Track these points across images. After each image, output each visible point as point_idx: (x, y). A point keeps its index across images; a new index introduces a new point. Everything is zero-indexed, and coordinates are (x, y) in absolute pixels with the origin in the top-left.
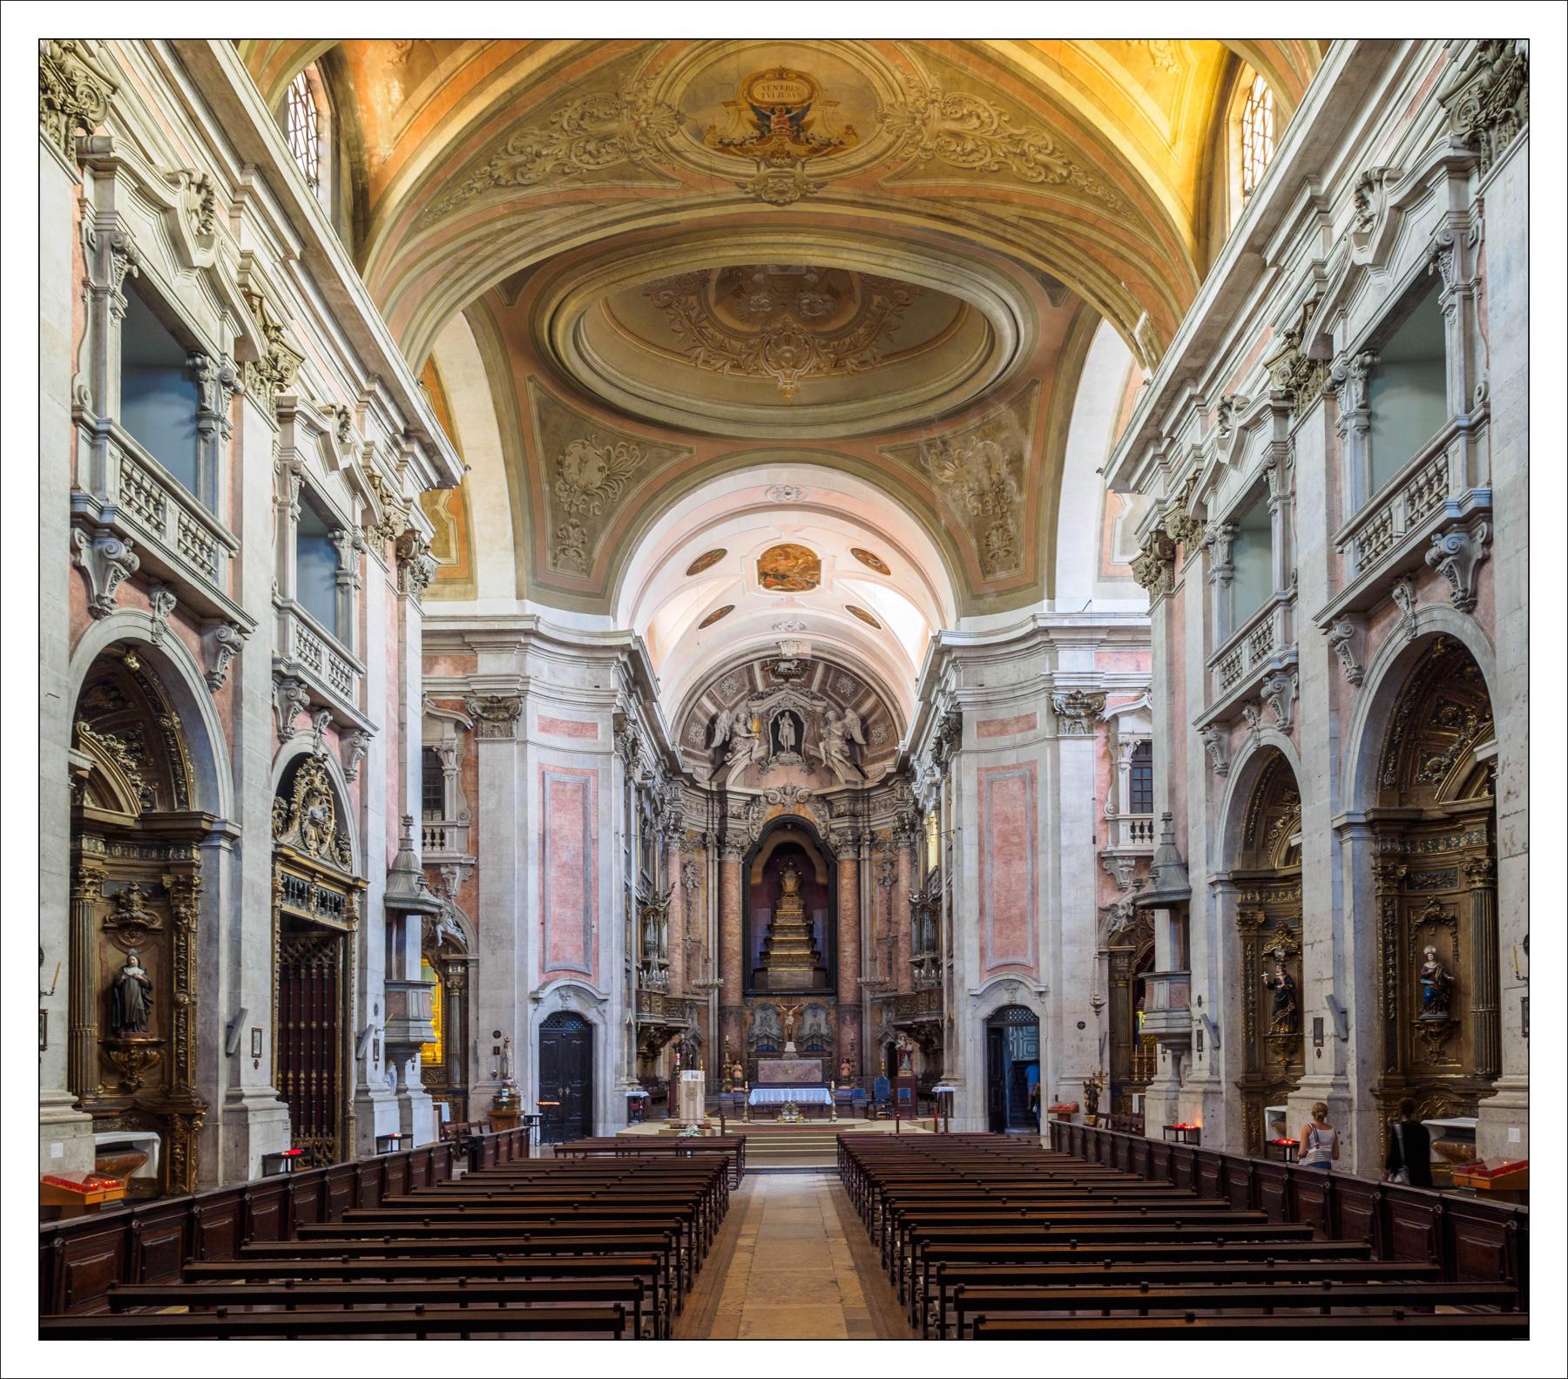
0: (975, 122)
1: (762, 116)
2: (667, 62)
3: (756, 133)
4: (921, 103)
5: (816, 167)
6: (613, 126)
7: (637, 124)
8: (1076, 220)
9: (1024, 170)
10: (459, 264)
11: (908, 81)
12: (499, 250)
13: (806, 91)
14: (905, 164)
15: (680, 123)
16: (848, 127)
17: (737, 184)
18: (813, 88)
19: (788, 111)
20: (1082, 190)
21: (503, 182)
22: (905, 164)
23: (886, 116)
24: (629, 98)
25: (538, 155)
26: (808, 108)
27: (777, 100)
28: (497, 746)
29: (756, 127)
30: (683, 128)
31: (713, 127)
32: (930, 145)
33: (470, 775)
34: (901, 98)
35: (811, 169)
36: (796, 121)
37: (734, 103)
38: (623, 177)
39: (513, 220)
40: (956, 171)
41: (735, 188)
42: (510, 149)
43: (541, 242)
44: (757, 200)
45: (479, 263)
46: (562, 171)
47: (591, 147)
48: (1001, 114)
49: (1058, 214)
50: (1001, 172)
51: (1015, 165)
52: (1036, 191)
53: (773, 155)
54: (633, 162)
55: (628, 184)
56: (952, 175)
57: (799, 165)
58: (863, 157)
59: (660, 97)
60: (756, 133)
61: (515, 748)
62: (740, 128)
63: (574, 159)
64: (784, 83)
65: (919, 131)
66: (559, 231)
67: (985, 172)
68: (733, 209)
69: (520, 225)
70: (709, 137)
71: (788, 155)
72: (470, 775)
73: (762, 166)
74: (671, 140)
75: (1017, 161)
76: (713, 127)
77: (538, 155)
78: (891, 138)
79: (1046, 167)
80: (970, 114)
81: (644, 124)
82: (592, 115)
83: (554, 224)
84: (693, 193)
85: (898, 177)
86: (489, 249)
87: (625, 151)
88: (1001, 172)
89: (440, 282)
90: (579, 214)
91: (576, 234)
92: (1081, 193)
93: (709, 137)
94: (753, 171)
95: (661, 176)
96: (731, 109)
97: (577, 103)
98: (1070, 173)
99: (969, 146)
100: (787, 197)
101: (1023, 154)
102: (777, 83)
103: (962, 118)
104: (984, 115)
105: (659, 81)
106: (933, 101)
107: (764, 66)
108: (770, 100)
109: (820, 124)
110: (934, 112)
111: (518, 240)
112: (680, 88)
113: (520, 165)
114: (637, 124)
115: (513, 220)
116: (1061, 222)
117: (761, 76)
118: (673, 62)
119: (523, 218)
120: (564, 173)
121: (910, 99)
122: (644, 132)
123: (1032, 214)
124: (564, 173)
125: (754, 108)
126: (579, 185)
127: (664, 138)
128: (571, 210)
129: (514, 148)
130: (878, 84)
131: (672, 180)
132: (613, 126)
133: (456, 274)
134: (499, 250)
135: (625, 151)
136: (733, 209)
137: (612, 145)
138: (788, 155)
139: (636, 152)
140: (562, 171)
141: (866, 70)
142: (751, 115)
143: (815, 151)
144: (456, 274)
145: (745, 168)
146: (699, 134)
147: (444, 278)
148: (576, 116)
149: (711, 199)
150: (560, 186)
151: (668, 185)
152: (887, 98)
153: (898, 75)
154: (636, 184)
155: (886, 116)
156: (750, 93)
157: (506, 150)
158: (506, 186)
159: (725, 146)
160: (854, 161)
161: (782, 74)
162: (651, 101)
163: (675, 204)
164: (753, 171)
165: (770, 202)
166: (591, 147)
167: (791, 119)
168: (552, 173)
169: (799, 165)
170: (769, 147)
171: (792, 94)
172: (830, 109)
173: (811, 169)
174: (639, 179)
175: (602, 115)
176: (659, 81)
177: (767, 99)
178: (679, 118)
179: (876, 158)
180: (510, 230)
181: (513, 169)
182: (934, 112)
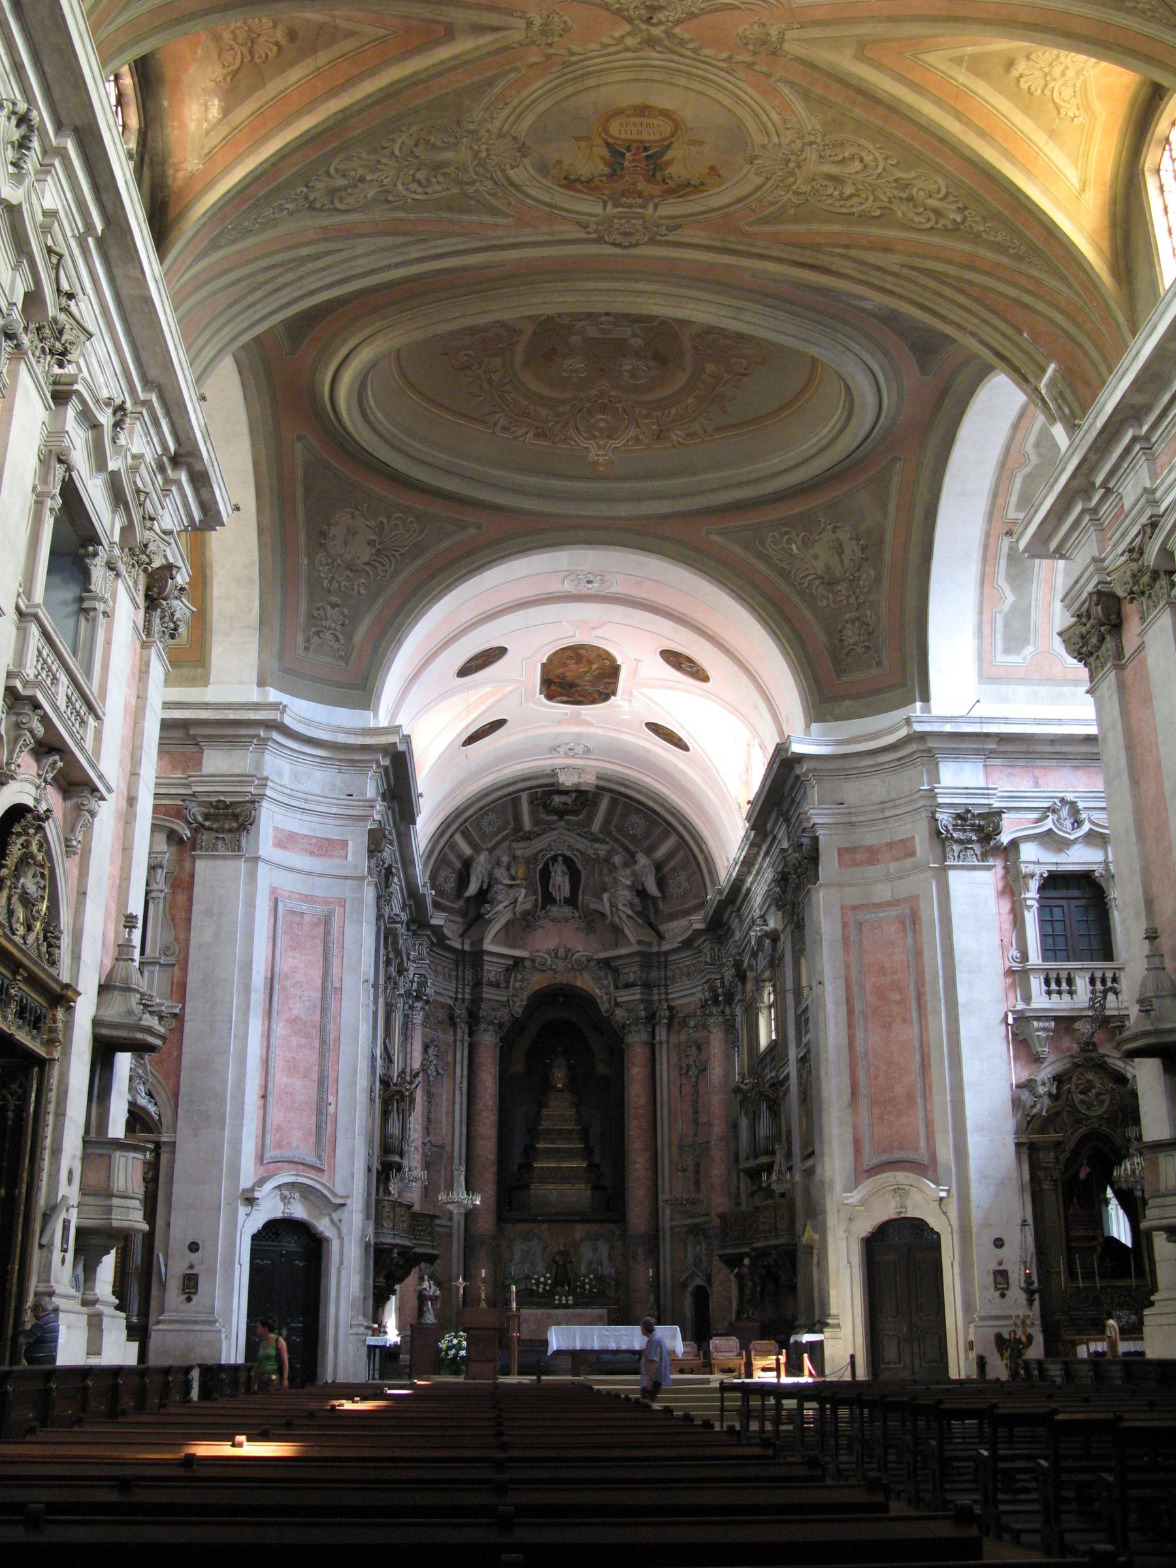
0: (857, 166)
1: (616, 154)
2: (518, 93)
3: (607, 170)
4: (798, 145)
5: (671, 209)
6: (449, 155)
7: (476, 155)
8: (972, 268)
9: (911, 215)
10: (254, 289)
11: (785, 121)
12: (301, 278)
13: (667, 128)
14: (772, 208)
15: (524, 156)
16: (712, 168)
17: (579, 224)
18: (678, 126)
19: (646, 149)
20: (978, 236)
21: (318, 205)
22: (772, 208)
23: (756, 157)
24: (471, 127)
25: (362, 180)
26: (668, 147)
27: (635, 137)
28: (218, 863)
29: (607, 163)
30: (526, 161)
31: (559, 162)
32: (803, 189)
33: (181, 898)
34: (775, 139)
35: (663, 211)
36: (653, 160)
37: (587, 138)
38: (451, 209)
39: (322, 247)
40: (831, 216)
41: (577, 228)
42: (332, 172)
43: (348, 274)
44: (599, 240)
45: (275, 291)
46: (385, 198)
47: (421, 175)
48: (886, 158)
49: (949, 262)
50: (884, 217)
51: (900, 210)
52: (925, 238)
53: (623, 195)
54: (465, 195)
55: (456, 217)
56: (826, 221)
57: (651, 206)
58: (726, 199)
59: (506, 128)
60: (607, 170)
61: (243, 866)
62: (590, 164)
63: (400, 187)
64: (645, 120)
65: (792, 174)
66: (370, 263)
67: (865, 218)
68: (571, 250)
69: (331, 253)
70: (554, 172)
71: (640, 195)
72: (181, 898)
73: (609, 206)
74: (511, 173)
75: (903, 207)
76: (559, 162)
77: (362, 180)
78: (759, 180)
79: (938, 213)
80: (852, 157)
81: (484, 154)
82: (427, 142)
83: (367, 255)
84: (528, 231)
85: (765, 221)
86: (290, 276)
87: (458, 182)
88: (884, 217)
89: (230, 306)
90: (395, 246)
91: (389, 267)
92: (977, 238)
93: (554, 172)
94: (598, 210)
95: (493, 211)
96: (582, 144)
97: (414, 129)
98: (964, 219)
99: (848, 190)
100: (633, 240)
101: (911, 199)
102: (637, 120)
103: (843, 161)
104: (868, 159)
105: (507, 111)
106: (811, 143)
107: (625, 102)
108: (628, 137)
109: (681, 163)
110: (811, 154)
111: (323, 269)
112: (529, 119)
113: (340, 189)
114: (476, 155)
115: (322, 247)
116: (952, 270)
117: (620, 112)
118: (525, 93)
119: (332, 246)
120: (387, 201)
121: (785, 141)
122: (482, 163)
123: (918, 262)
124: (387, 201)
125: (608, 145)
126: (401, 215)
127: (503, 171)
128: (389, 241)
129: (337, 170)
130: (750, 123)
131: (507, 215)
132: (449, 155)
133: (250, 299)
134: (301, 278)
135: (458, 182)
136: (571, 250)
137: (445, 175)
138: (640, 195)
139: (472, 183)
140: (385, 198)
141: (740, 111)
142: (605, 152)
143: (671, 192)
144: (250, 299)
145: (590, 207)
146: (543, 169)
147: (235, 302)
148: (411, 142)
149: (547, 238)
150: (379, 215)
151: (502, 221)
152: (760, 139)
153: (774, 116)
154: (465, 218)
155: (756, 157)
156: (605, 130)
157: (328, 173)
158: (321, 210)
159: (569, 183)
160: (714, 203)
161: (643, 111)
162: (495, 131)
163: (505, 242)
164: (598, 210)
165: (614, 244)
166: (421, 175)
167: (648, 157)
168: (374, 199)
169: (651, 206)
170: (620, 186)
171: (653, 131)
172: (693, 149)
173: (663, 211)
174: (469, 212)
175: (439, 143)
176: (507, 111)
177: (623, 136)
178: (523, 151)
179: (740, 201)
180: (317, 257)
181: (332, 192)
182: (811, 154)
